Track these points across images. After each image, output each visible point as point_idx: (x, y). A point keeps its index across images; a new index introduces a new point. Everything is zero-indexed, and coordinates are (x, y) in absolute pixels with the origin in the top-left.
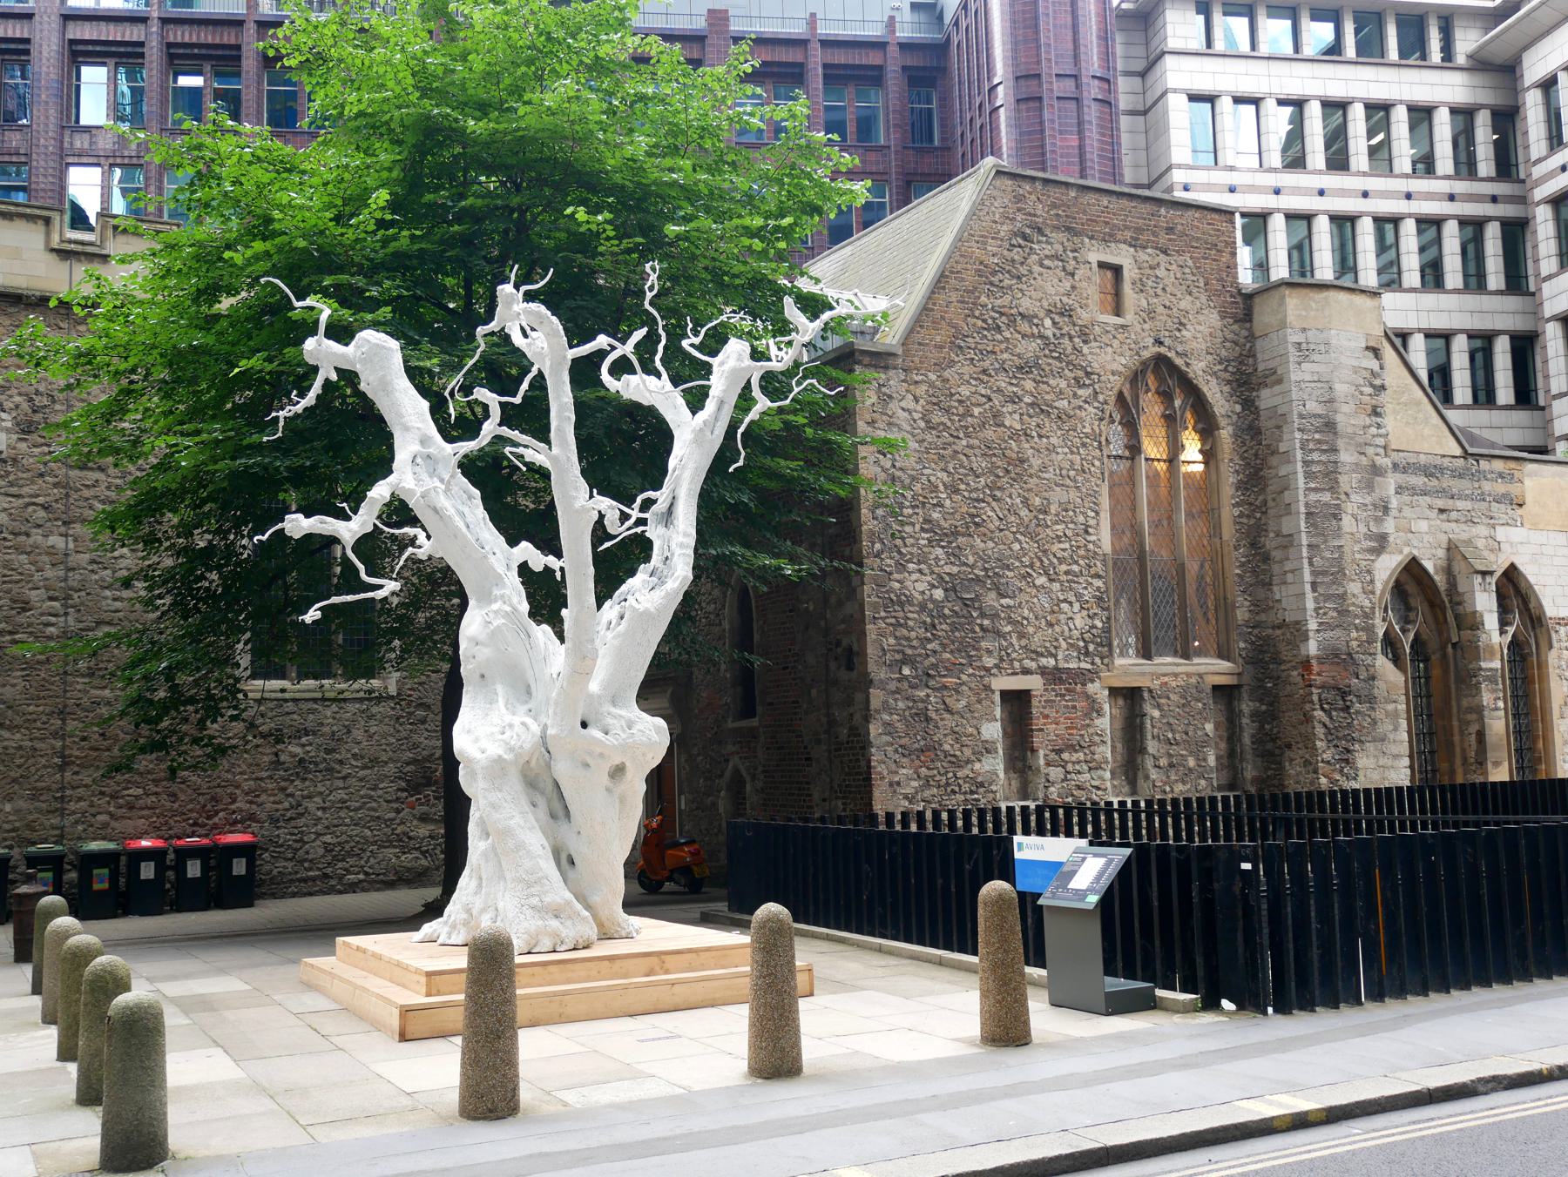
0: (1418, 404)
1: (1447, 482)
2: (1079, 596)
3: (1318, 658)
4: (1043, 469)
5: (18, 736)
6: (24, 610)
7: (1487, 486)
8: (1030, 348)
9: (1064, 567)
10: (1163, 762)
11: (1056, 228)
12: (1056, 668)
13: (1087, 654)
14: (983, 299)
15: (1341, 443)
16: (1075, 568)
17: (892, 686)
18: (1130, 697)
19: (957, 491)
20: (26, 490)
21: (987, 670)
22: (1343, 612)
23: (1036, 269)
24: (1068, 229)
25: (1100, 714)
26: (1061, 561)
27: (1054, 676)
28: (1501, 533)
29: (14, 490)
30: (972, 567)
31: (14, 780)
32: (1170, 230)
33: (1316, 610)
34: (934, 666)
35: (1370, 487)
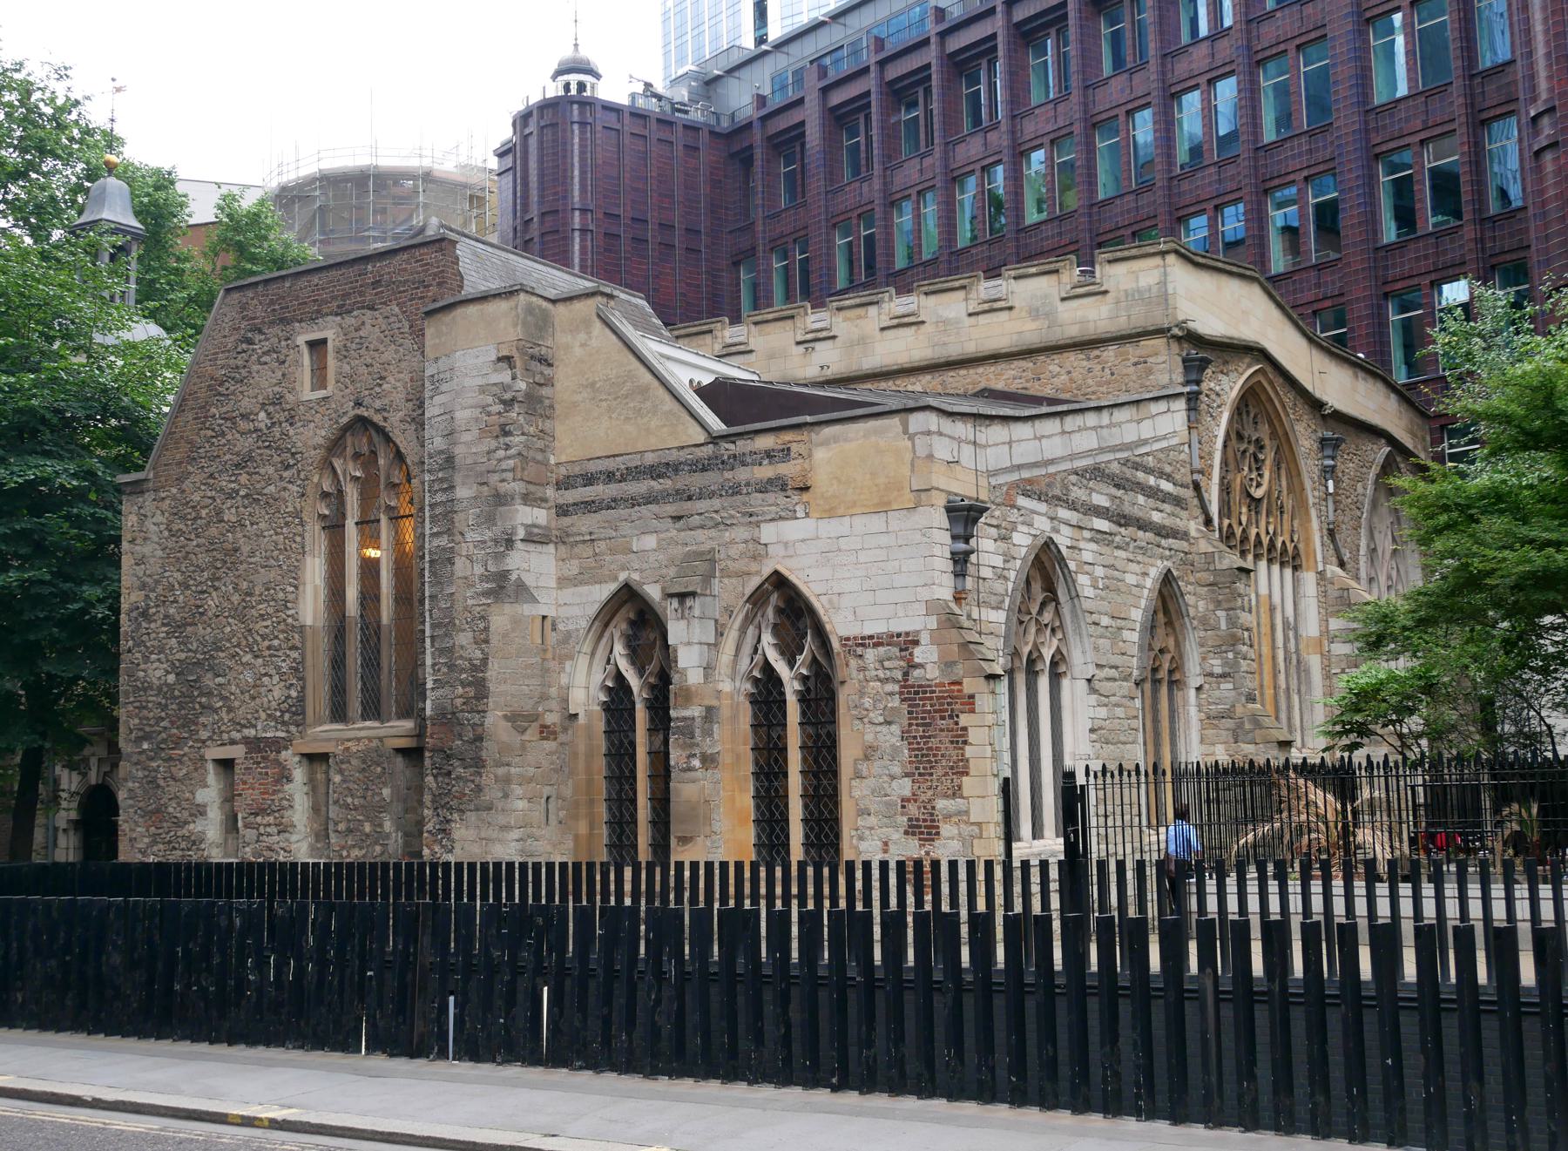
0: (644, 391)
1: (686, 480)
2: (278, 668)
3: (432, 718)
4: (252, 553)
7: (742, 474)
8: (245, 444)
9: (266, 643)
10: (342, 827)
11: (272, 323)
12: (256, 738)
13: (284, 723)
14: (213, 410)
15: (458, 479)
16: (276, 642)
17: (135, 758)
19: (188, 587)
21: (204, 742)
22: (451, 667)
23: (255, 368)
24: (282, 320)
25: (289, 780)
26: (264, 637)
28: (768, 532)
30: (195, 652)
32: (376, 284)
33: (434, 665)
34: (164, 741)
35: (490, 520)
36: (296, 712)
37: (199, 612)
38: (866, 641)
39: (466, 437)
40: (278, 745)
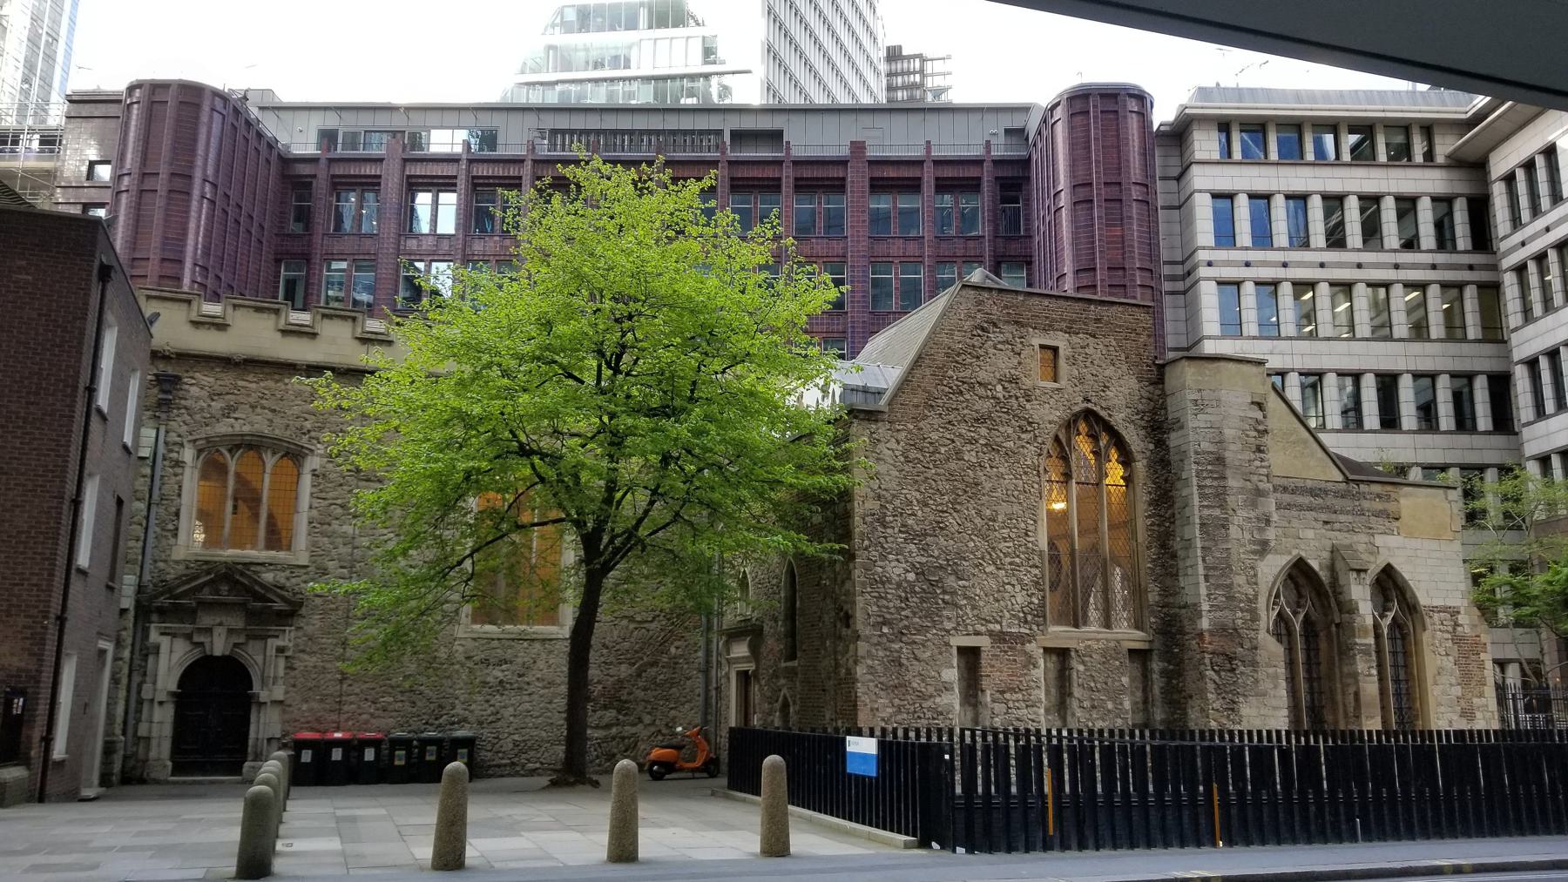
0: (1305, 442)
1: (1330, 500)
2: (1020, 581)
4: (994, 489)
7: (1366, 504)
8: (985, 406)
9: (1008, 560)
10: (1086, 704)
11: (1008, 322)
13: (1026, 622)
14: (950, 373)
15: (1228, 473)
17: (875, 640)
18: (1061, 655)
19: (927, 505)
20: (331, 495)
21: (948, 631)
22: (1230, 598)
23: (992, 351)
24: (1016, 323)
27: (1000, 638)
29: (323, 495)
32: (1098, 320)
34: (906, 627)
35: (1254, 505)
36: (1039, 616)
37: (940, 527)
38: (1434, 609)
39: (1232, 447)
40: (1023, 639)
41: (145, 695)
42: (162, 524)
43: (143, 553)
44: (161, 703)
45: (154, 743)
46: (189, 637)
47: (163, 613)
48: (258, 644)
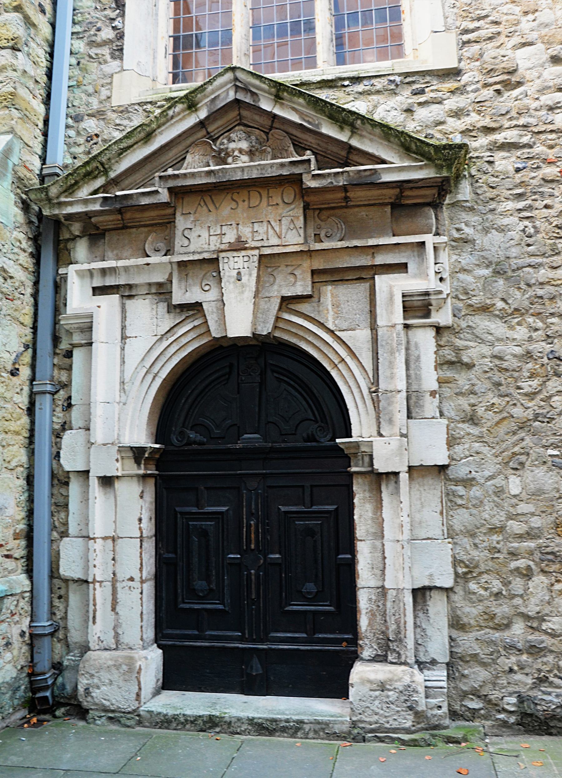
5: (521, 333)
6: (509, 85)
31: (523, 425)
41: (69, 462)
42: (84, 30)
43: (47, 100)
44: (107, 482)
45: (101, 595)
46: (162, 291)
47: (96, 232)
48: (351, 296)
